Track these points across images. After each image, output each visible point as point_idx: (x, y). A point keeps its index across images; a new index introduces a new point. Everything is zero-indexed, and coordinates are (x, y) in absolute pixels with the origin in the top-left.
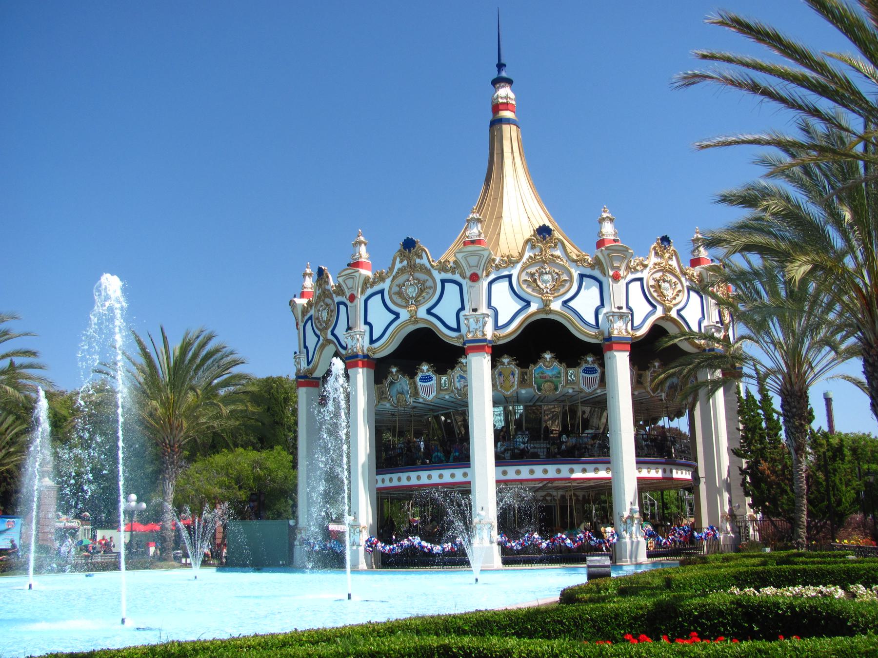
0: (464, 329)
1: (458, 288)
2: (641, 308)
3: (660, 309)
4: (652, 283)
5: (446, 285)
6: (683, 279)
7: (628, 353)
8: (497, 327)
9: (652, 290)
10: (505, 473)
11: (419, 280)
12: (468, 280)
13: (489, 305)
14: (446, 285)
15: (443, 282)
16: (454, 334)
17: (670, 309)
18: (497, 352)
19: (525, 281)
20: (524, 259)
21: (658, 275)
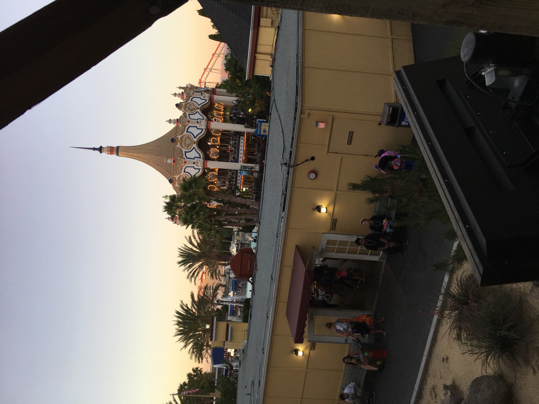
0: (200, 167)
1: (187, 168)
2: (197, 116)
3: (198, 110)
4: (190, 111)
5: (185, 171)
6: (188, 102)
8: (200, 158)
9: (192, 112)
10: (241, 161)
14: (185, 171)
16: (201, 171)
17: (198, 108)
18: (207, 158)
19: (187, 148)
21: (187, 109)
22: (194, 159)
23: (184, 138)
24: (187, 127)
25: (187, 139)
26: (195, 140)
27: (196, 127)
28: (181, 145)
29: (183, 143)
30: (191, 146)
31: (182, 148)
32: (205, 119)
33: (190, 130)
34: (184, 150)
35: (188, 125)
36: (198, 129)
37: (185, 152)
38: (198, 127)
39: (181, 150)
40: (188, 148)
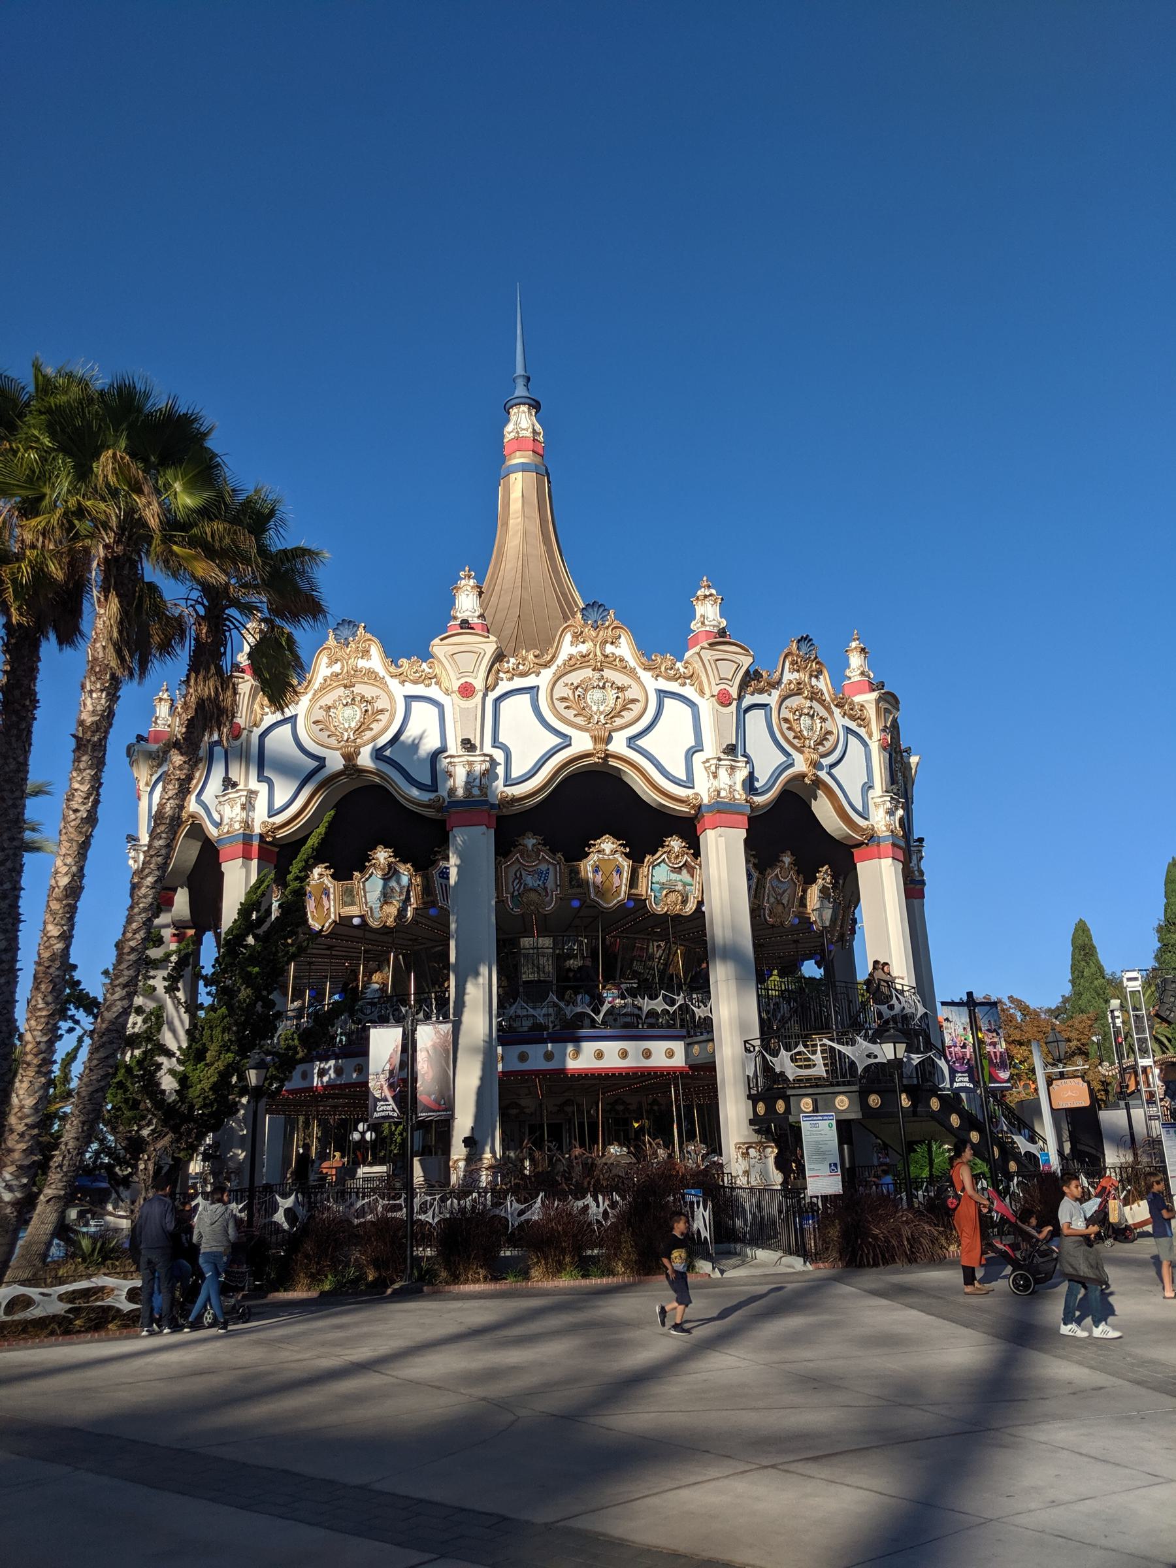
7: (742, 834)
11: (363, 699)
12: (456, 697)
13: (496, 743)
15: (409, 699)
19: (563, 699)
20: (559, 661)
22: (496, 743)
23: (620, 679)
24: (689, 691)
25: (612, 694)
26: (618, 745)
27: (698, 747)
28: (573, 664)
29: (588, 673)
30: (580, 720)
31: (554, 668)
32: (759, 800)
33: (676, 714)
34: (544, 679)
35: (702, 693)
36: (690, 754)
37: (533, 690)
38: (698, 758)
39: (546, 665)
40: (560, 706)
